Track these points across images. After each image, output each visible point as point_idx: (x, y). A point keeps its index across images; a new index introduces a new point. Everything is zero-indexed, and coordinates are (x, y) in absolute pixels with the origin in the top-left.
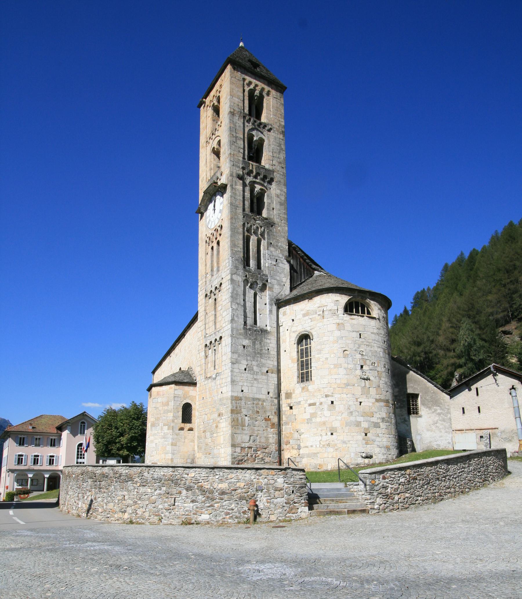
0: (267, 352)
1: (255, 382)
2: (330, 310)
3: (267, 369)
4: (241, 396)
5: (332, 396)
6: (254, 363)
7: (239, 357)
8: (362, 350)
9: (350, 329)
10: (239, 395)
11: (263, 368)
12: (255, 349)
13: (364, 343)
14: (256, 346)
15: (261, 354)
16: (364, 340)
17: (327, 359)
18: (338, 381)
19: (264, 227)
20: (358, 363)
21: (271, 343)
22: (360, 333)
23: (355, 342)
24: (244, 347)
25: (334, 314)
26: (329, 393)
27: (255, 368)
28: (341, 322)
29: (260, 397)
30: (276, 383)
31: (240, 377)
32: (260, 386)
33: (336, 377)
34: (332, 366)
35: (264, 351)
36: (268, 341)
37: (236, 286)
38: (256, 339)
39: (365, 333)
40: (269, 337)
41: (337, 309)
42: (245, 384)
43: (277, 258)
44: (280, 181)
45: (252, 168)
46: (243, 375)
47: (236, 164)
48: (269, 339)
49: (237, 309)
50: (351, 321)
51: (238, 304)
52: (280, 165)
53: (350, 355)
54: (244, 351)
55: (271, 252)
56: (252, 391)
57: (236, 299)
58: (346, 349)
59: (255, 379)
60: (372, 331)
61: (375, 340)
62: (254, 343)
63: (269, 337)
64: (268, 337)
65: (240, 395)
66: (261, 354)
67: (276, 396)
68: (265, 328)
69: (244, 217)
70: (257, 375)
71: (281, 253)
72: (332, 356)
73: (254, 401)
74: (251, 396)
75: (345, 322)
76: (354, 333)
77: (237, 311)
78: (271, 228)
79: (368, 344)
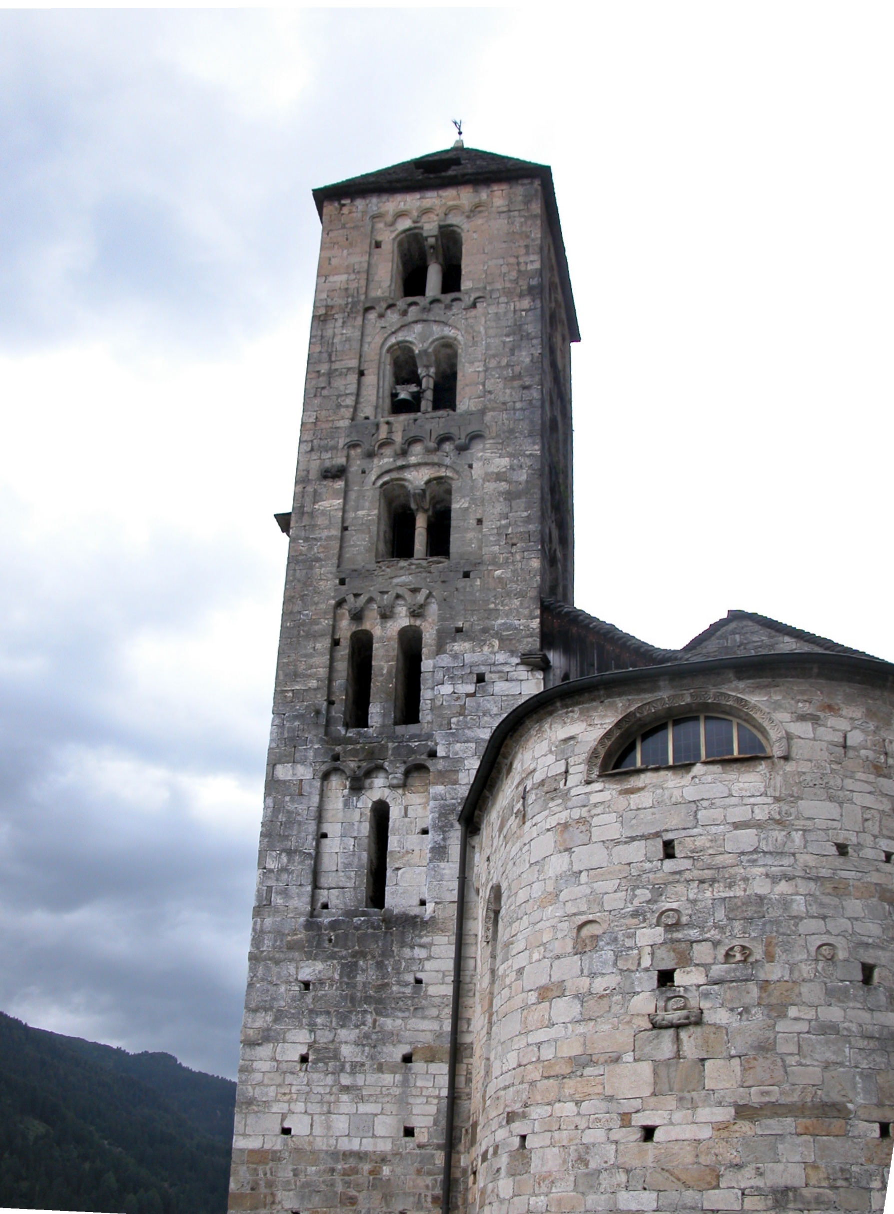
0: (408, 991)
1: (344, 1097)
2: (542, 783)
3: (406, 1049)
4: (278, 1147)
5: (524, 1116)
6: (343, 1034)
7: (276, 1020)
8: (674, 906)
9: (615, 832)
10: (267, 1146)
11: (388, 1049)
12: (352, 986)
13: (688, 875)
14: (360, 978)
15: (379, 1001)
16: (687, 864)
17: (520, 971)
18: (547, 1053)
19: (428, 587)
20: (646, 962)
21: (429, 958)
22: (668, 836)
23: (633, 883)
24: (307, 985)
25: (553, 795)
26: (517, 1107)
27: (346, 1051)
28: (576, 814)
29: (363, 1149)
30: (445, 1092)
31: (279, 1085)
32: (364, 1108)
33: (541, 1035)
34: (533, 997)
35: (395, 988)
36: (420, 953)
37: (287, 798)
38: (362, 954)
39: (695, 831)
40: (425, 940)
41: (563, 769)
42: (299, 1107)
43: (483, 669)
44: (511, 431)
45: (390, 432)
46: (289, 1079)
47: (323, 443)
48: (422, 946)
49: (284, 870)
50: (622, 802)
51: (290, 853)
52: (516, 383)
53: (606, 938)
54: (302, 997)
55: (455, 657)
56: (329, 1127)
57: (287, 837)
58: (591, 917)
59: (346, 1089)
60: (739, 814)
61: (755, 851)
62: (350, 970)
63: (425, 940)
64: (418, 940)
65: (276, 1143)
66: (379, 1001)
67: (442, 1141)
68: (416, 910)
69: (342, 582)
70: (353, 1073)
71: (501, 648)
72: (536, 956)
73: (337, 1161)
74: (321, 1144)
75: (593, 812)
76: (636, 843)
77: (285, 876)
78: (462, 583)
79: (707, 874)
